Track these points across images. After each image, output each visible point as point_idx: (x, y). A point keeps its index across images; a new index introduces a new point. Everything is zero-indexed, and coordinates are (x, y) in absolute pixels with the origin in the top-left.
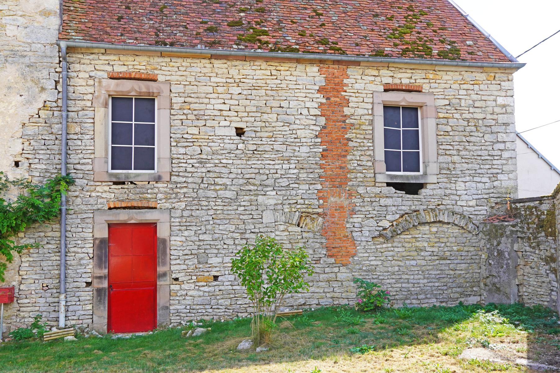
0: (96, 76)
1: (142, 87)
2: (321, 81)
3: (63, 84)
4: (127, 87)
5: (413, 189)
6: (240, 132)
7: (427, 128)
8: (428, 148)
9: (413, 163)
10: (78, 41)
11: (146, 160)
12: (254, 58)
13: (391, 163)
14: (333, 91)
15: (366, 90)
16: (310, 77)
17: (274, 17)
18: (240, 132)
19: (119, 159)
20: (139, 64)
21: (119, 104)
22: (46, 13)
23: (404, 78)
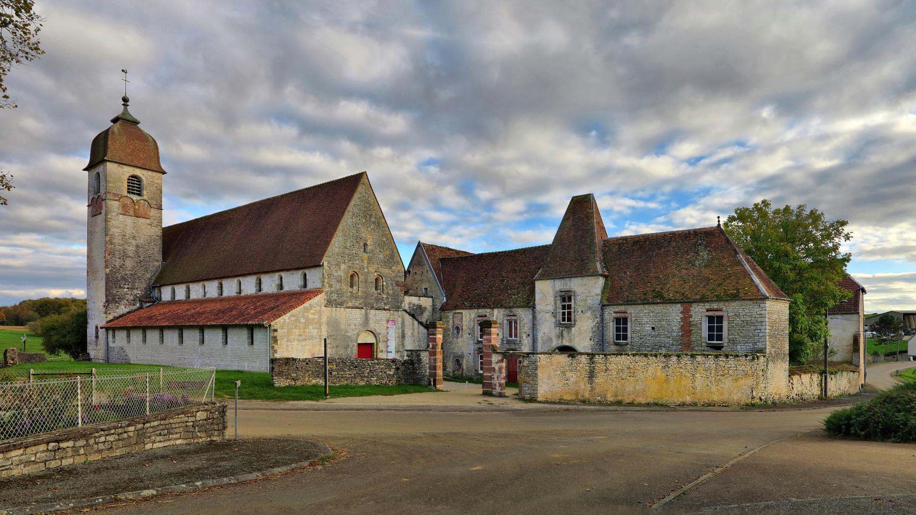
0: (610, 314)
1: (623, 315)
2: (681, 309)
3: (602, 316)
4: (618, 315)
5: (719, 348)
6: (653, 328)
7: (725, 324)
8: (725, 333)
9: (720, 338)
10: (606, 303)
11: (625, 337)
12: (657, 303)
13: (711, 337)
14: (686, 314)
15: (699, 313)
16: (679, 308)
17: (668, 286)
18: (653, 328)
19: (618, 337)
20: (622, 308)
21: (618, 321)
22: (597, 295)
23: (715, 306)
